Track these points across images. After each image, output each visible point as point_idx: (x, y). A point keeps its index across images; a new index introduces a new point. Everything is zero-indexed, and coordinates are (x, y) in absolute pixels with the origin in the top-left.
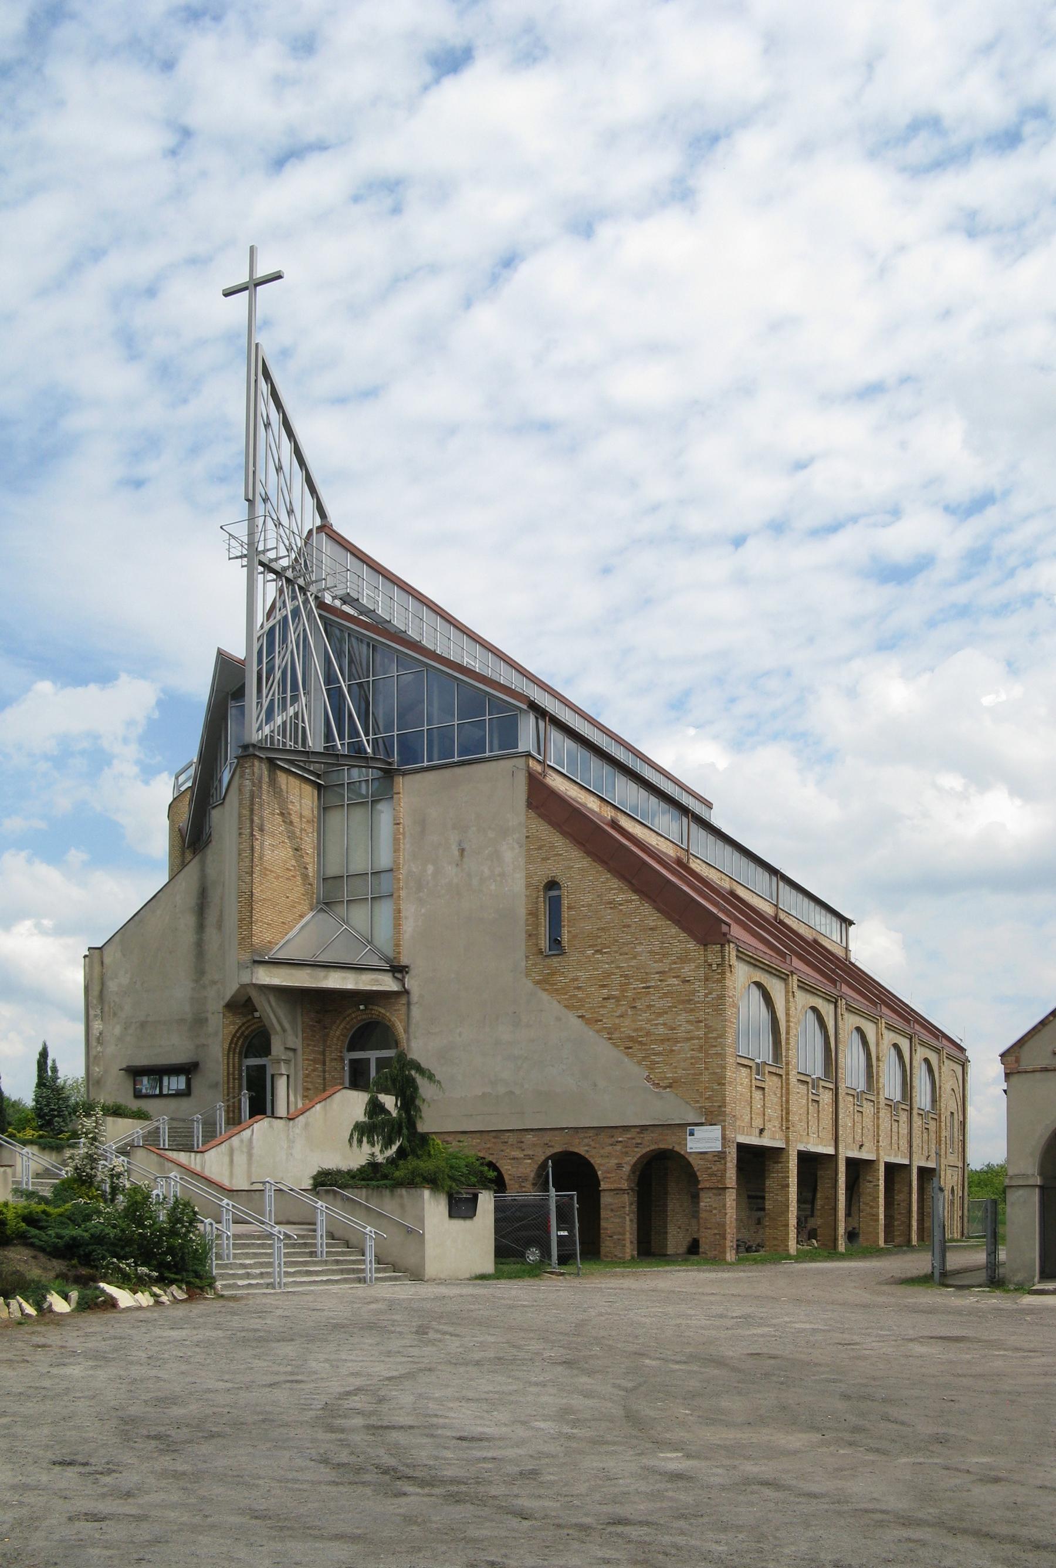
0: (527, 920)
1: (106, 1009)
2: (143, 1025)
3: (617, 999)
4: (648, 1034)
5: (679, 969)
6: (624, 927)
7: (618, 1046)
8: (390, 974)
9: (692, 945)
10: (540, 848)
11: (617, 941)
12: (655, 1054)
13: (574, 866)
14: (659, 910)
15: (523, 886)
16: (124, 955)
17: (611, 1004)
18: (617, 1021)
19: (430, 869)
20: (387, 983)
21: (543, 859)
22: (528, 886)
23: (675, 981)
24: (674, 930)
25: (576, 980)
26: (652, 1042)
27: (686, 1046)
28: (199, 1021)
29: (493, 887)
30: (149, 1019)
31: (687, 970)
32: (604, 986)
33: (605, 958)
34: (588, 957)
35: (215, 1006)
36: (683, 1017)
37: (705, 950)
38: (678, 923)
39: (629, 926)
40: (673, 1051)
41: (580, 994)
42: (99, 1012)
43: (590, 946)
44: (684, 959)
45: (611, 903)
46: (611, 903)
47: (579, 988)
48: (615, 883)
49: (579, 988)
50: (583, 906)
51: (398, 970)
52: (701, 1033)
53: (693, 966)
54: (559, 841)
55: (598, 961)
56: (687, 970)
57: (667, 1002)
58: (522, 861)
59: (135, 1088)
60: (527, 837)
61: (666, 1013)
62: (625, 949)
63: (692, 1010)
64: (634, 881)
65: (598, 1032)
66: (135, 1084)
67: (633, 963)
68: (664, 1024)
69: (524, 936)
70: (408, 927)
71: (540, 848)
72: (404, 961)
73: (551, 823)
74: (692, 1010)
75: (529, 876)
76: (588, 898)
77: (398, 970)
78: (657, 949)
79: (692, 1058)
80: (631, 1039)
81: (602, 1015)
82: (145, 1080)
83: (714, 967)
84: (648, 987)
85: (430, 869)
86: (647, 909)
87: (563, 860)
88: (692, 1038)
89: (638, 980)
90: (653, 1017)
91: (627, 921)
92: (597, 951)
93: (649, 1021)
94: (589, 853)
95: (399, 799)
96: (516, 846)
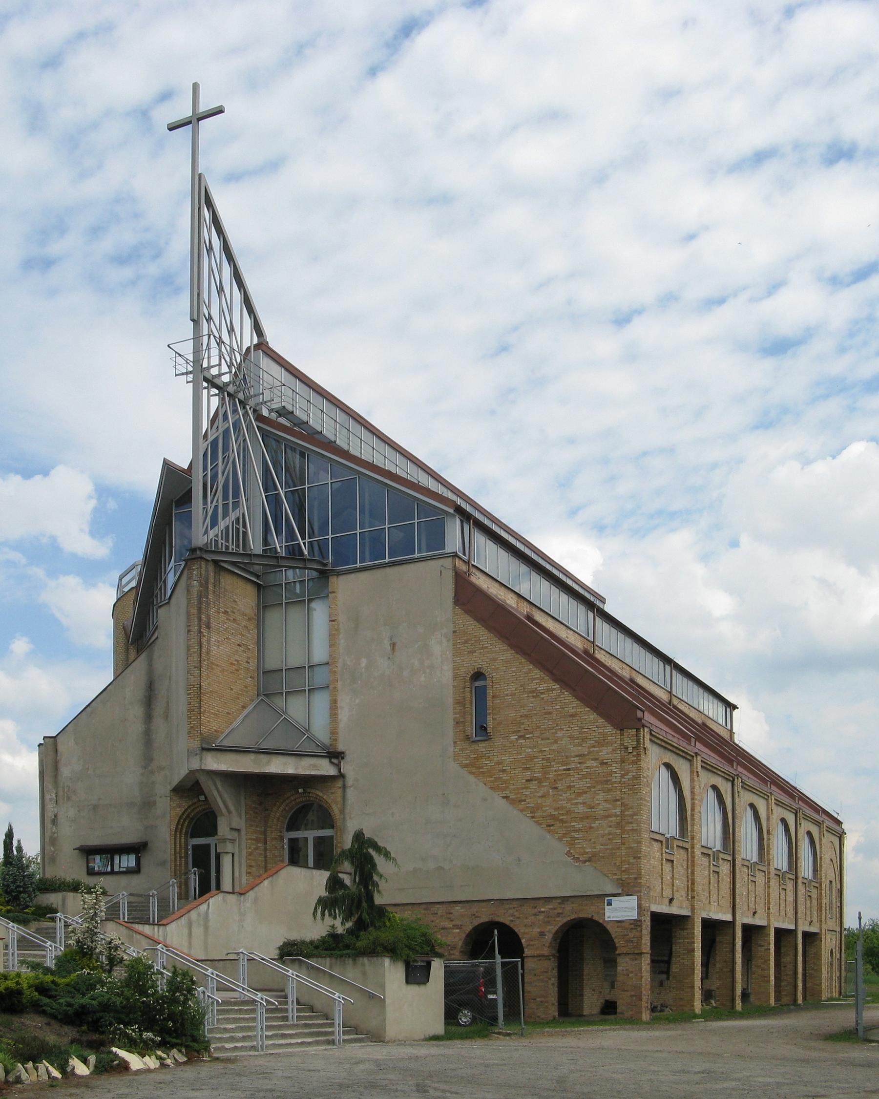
0: (454, 709)
1: (61, 793)
2: (95, 808)
3: (540, 781)
4: (569, 812)
5: (598, 752)
6: (546, 713)
7: (540, 824)
9: (609, 729)
10: (466, 642)
11: (539, 727)
12: (575, 831)
14: (578, 698)
15: (451, 677)
17: (533, 785)
18: (539, 801)
19: (364, 662)
20: (325, 768)
21: (470, 652)
24: (593, 716)
25: (501, 763)
27: (604, 823)
28: (147, 805)
29: (423, 679)
31: (605, 753)
34: (512, 742)
35: (163, 789)
36: (601, 796)
37: (622, 735)
38: (595, 709)
39: (550, 713)
40: (591, 828)
41: (505, 777)
44: (602, 742)
45: (533, 692)
46: (533, 692)
47: (504, 771)
48: (537, 673)
49: (504, 771)
51: (335, 756)
53: (610, 748)
54: (483, 634)
56: (605, 753)
58: (449, 654)
59: (88, 866)
60: (454, 632)
61: (586, 793)
62: (547, 735)
63: (609, 790)
65: (521, 811)
66: (88, 863)
67: (555, 747)
68: (584, 803)
69: (451, 723)
70: (344, 715)
71: (466, 642)
72: (341, 748)
75: (455, 668)
77: (335, 756)
78: (576, 734)
79: (610, 834)
80: (552, 817)
82: (98, 858)
84: (569, 769)
85: (364, 662)
90: (573, 796)
91: (549, 708)
92: (520, 737)
93: (569, 800)
96: (444, 640)
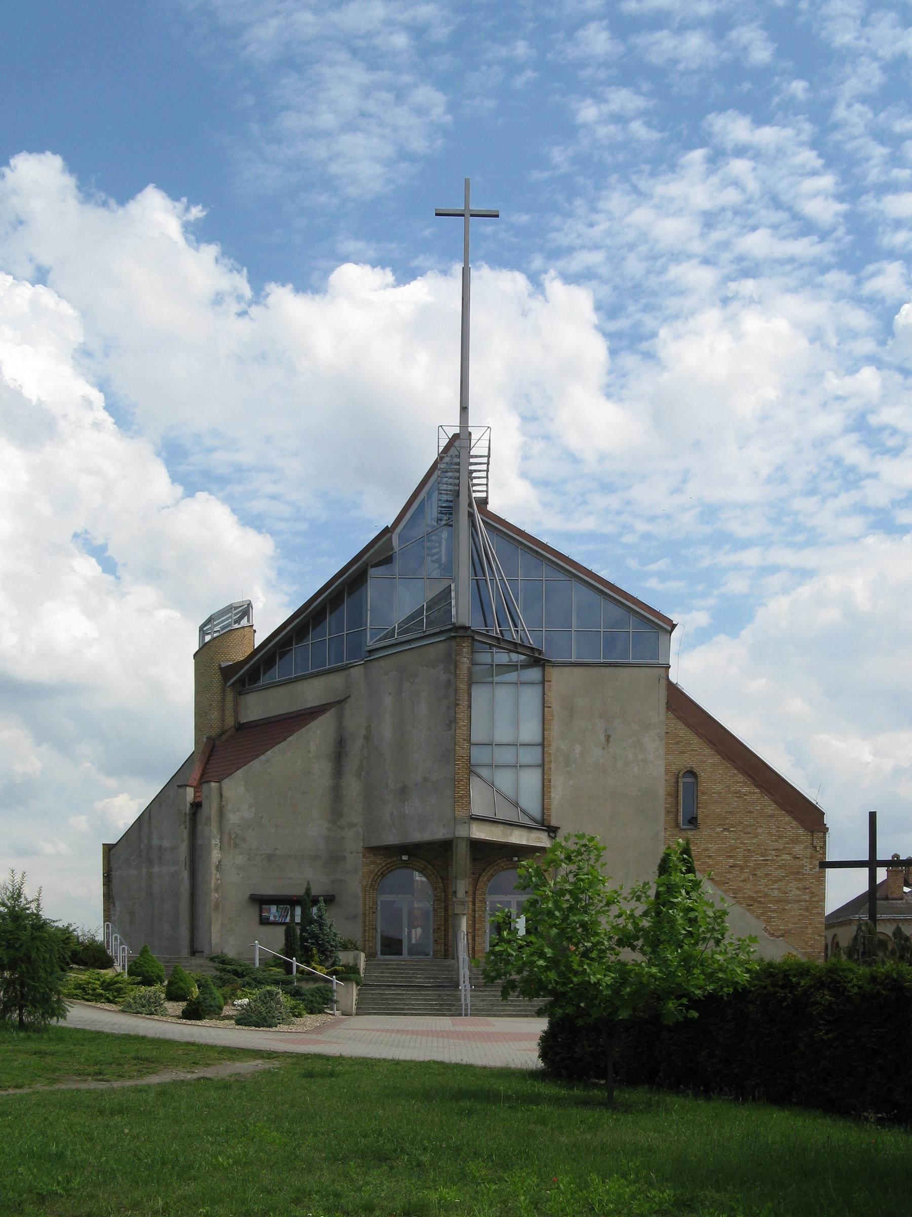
0: (666, 799)
1: (226, 838)
2: (270, 858)
3: (742, 868)
4: (766, 895)
5: (791, 848)
6: (748, 812)
7: (741, 904)
8: (546, 834)
9: (801, 831)
10: (677, 743)
11: (742, 823)
12: (771, 911)
13: (706, 761)
14: (775, 802)
15: (663, 772)
16: (247, 790)
17: (735, 871)
18: (741, 884)
19: (578, 748)
20: (540, 840)
21: (680, 752)
22: (667, 772)
23: (788, 857)
24: (788, 819)
25: (707, 850)
26: (770, 902)
27: (796, 906)
28: (335, 859)
29: (636, 770)
30: (277, 852)
31: (798, 849)
32: (730, 857)
33: (732, 835)
34: (717, 833)
35: (353, 845)
36: (793, 885)
37: (812, 836)
38: (789, 813)
39: (752, 812)
40: (785, 909)
41: (710, 862)
42: (218, 842)
43: (719, 825)
44: (795, 841)
45: (737, 793)
46: (737, 793)
47: (710, 857)
48: (740, 778)
49: (710, 857)
50: (714, 793)
51: (552, 831)
52: (807, 897)
53: (802, 846)
54: (694, 740)
55: (726, 837)
56: (798, 849)
57: (780, 873)
58: (662, 752)
59: (261, 916)
60: (667, 733)
61: (781, 880)
62: (749, 830)
63: (800, 880)
64: (756, 778)
65: (725, 891)
66: (261, 912)
67: (755, 840)
68: (779, 889)
69: (663, 812)
70: (557, 795)
71: (677, 743)
72: (554, 823)
73: (687, 725)
74: (800, 880)
75: (668, 764)
76: (718, 788)
77: (552, 831)
78: (774, 832)
79: (800, 915)
80: (752, 898)
81: (729, 879)
82: (274, 908)
83: (818, 849)
84: (767, 860)
85: (578, 748)
86: (766, 800)
87: (698, 755)
88: (800, 901)
89: (758, 854)
90: (770, 883)
91: (751, 809)
92: (725, 829)
93: (767, 886)
94: (719, 752)
95: (550, 686)
96: (656, 738)
